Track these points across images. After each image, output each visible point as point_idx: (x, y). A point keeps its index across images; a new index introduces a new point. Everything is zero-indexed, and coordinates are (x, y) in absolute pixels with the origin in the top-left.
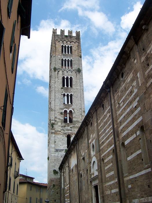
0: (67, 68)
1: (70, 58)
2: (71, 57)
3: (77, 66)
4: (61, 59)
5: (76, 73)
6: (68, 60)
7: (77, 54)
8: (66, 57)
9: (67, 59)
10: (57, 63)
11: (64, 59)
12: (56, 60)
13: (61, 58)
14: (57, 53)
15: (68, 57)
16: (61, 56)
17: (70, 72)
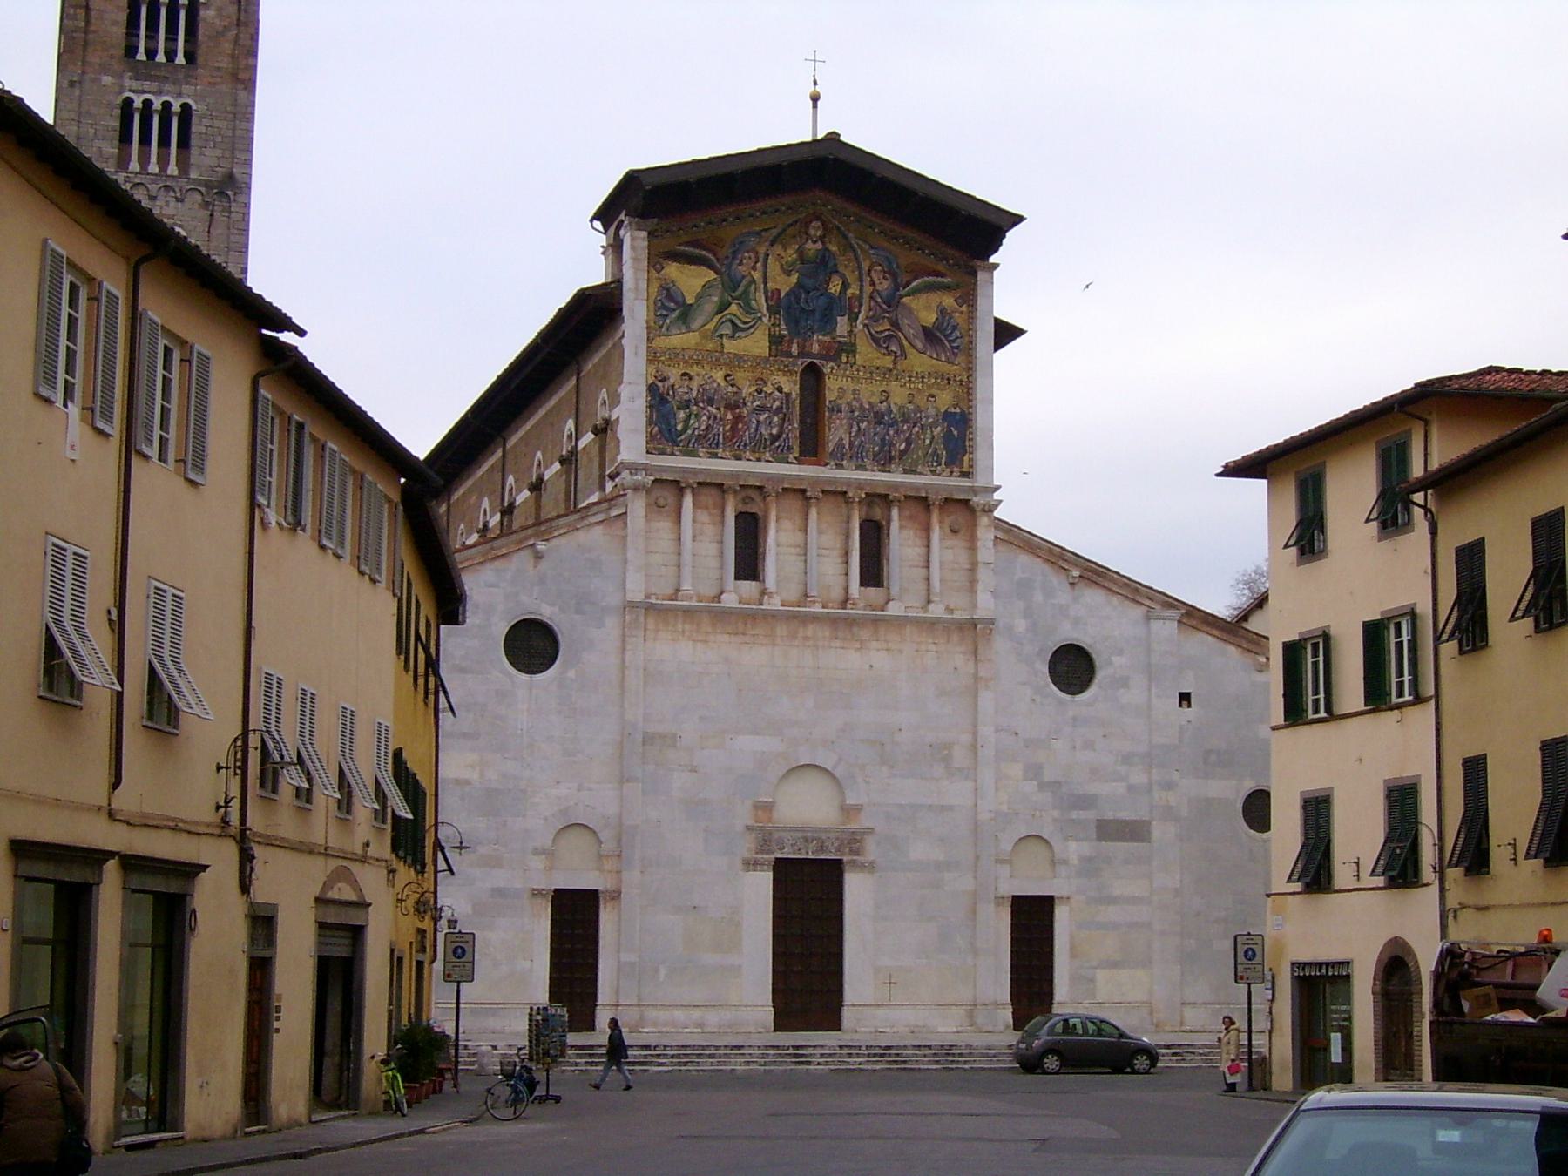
0: (154, 168)
1: (180, 95)
2: (186, 89)
3: (218, 152)
4: (119, 101)
5: (207, 204)
6: (167, 106)
7: (225, 63)
8: (154, 86)
9: (157, 105)
10: (92, 131)
11: (138, 103)
12: (84, 109)
13: (121, 93)
14: (95, 59)
15: (167, 87)
16: (121, 77)
17: (173, 203)
